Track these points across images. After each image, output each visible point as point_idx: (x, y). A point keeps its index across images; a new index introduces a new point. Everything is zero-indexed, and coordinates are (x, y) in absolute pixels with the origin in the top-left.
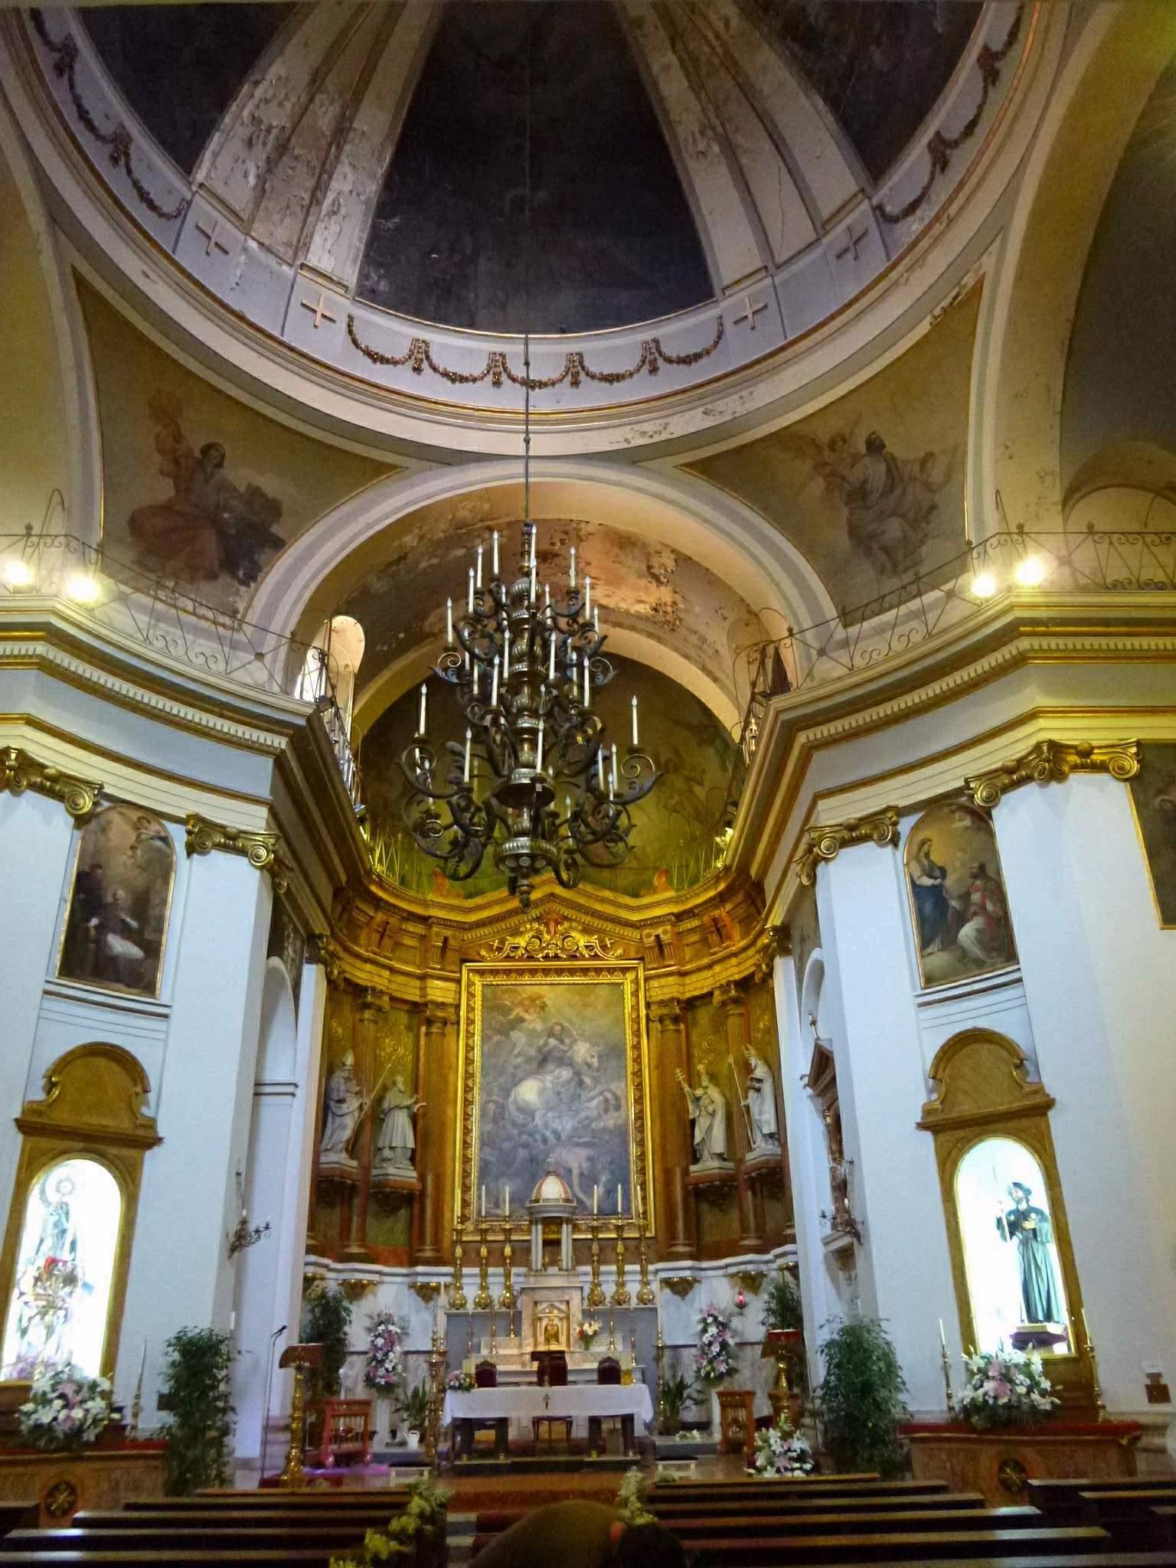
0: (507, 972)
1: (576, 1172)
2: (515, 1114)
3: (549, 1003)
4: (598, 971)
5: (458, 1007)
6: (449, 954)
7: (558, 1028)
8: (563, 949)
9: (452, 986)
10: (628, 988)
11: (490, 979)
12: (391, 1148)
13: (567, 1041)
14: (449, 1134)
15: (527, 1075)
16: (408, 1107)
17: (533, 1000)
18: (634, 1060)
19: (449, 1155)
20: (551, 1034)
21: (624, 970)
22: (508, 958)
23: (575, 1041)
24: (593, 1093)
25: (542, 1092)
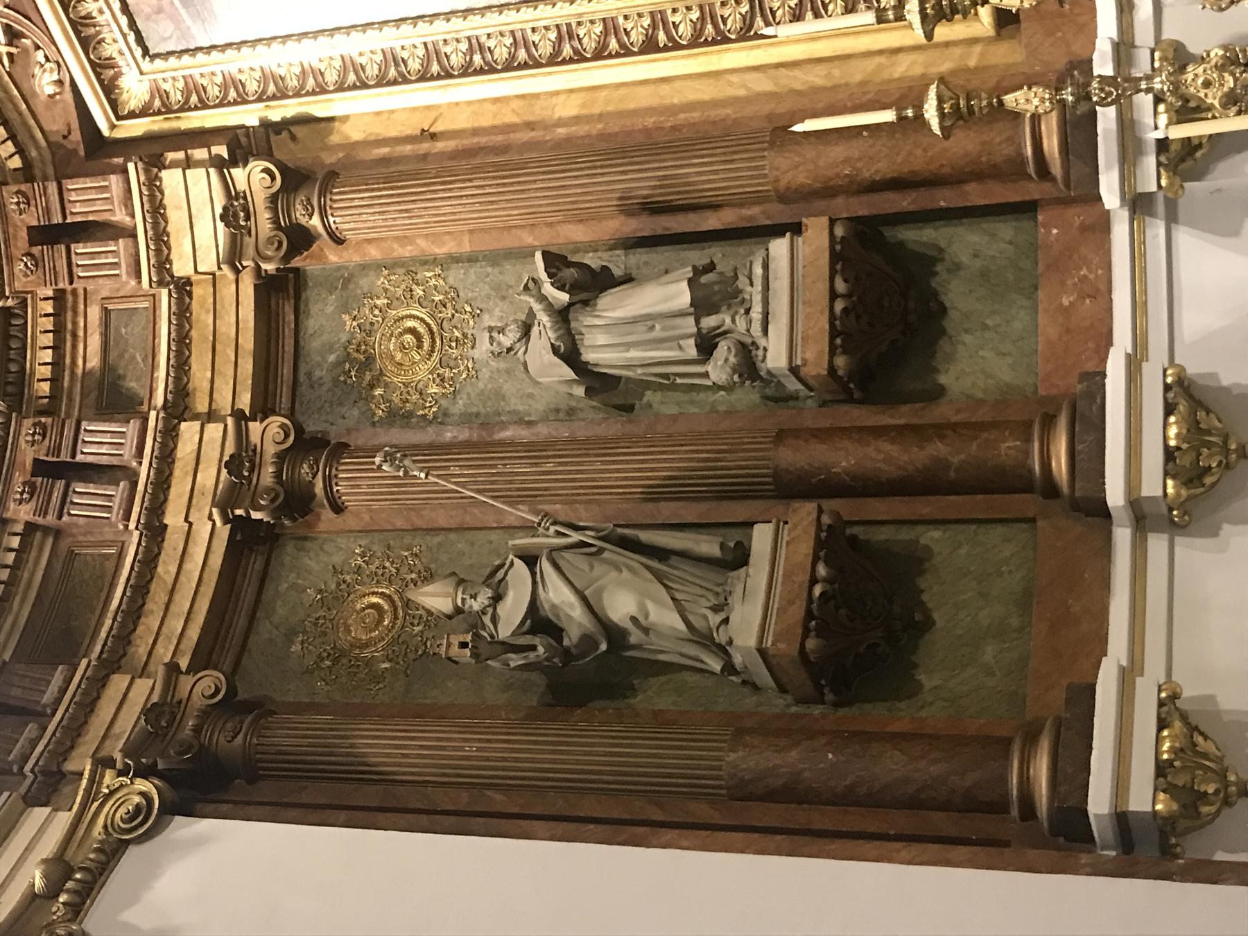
6: (79, 211)
9: (171, 179)
11: (115, 43)
12: (707, 345)
14: (644, 99)
16: (562, 316)
19: (705, 92)
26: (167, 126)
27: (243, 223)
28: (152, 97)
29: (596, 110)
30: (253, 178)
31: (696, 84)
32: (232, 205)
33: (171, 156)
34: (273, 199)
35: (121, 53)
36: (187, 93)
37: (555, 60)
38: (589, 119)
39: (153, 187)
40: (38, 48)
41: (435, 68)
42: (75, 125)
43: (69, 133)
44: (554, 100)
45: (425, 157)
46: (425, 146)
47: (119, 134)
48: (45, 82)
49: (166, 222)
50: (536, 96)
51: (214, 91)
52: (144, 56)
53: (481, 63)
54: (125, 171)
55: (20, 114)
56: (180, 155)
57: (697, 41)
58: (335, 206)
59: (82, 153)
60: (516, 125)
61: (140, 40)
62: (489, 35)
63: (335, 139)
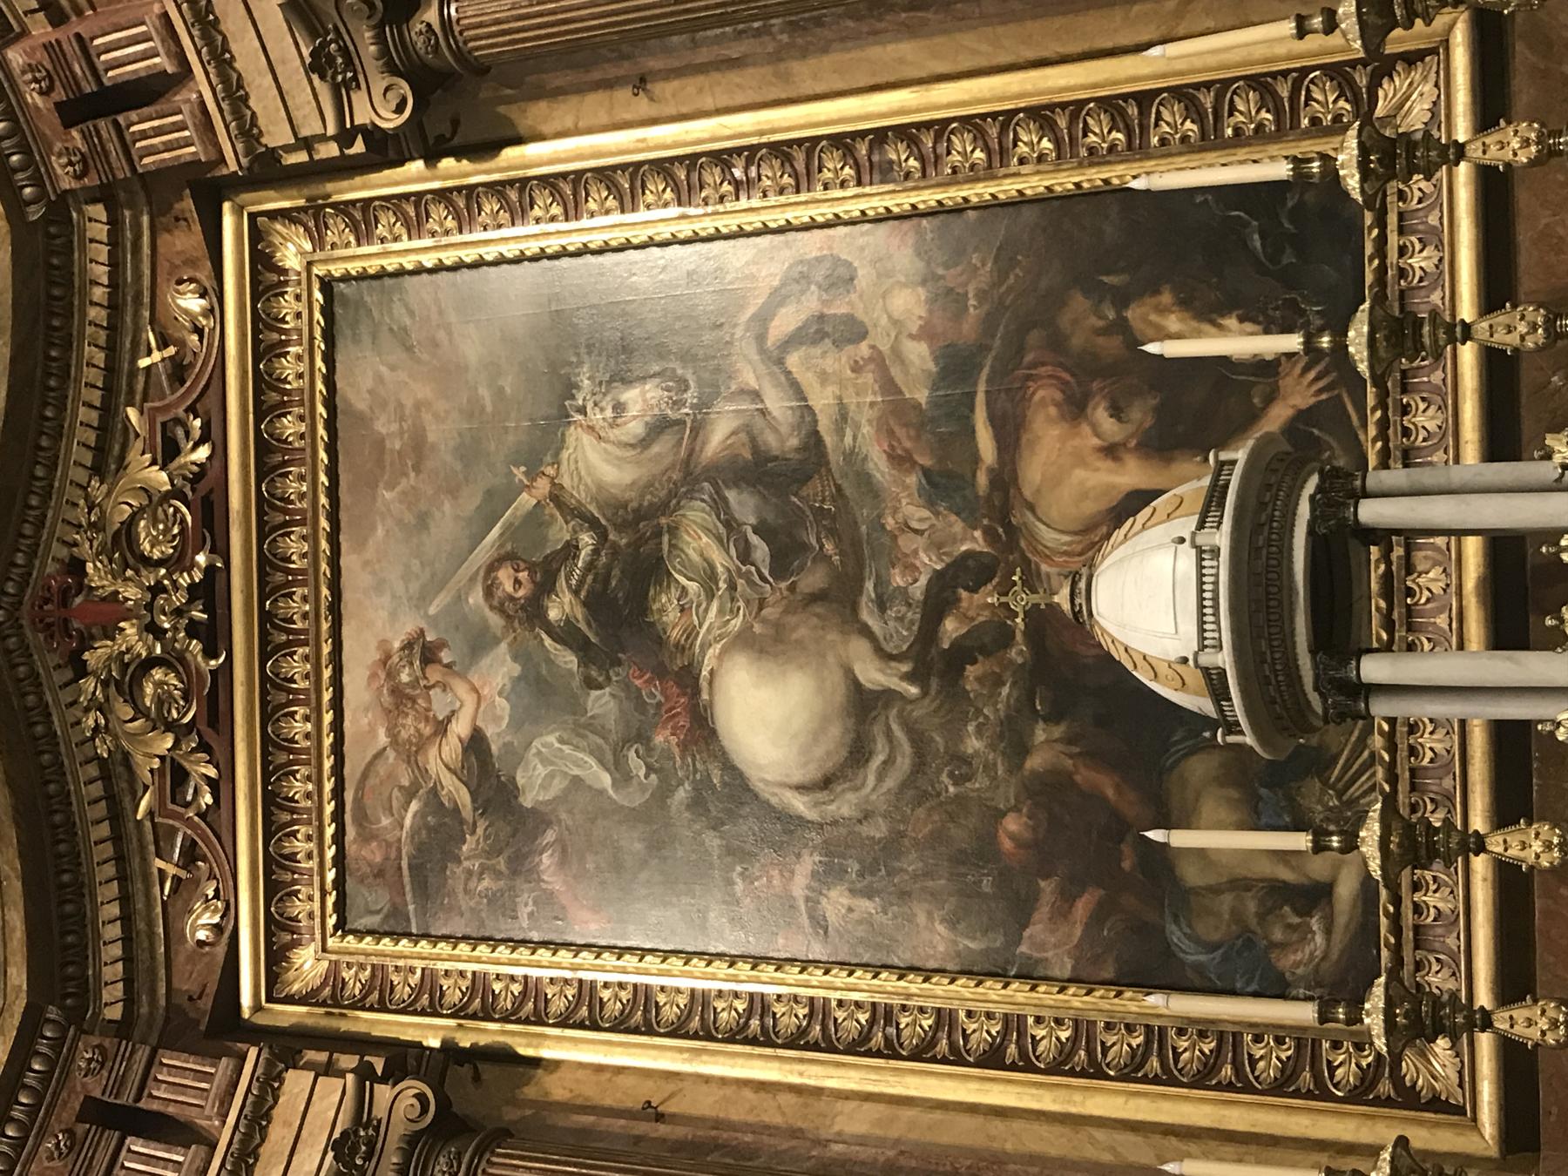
0: (273, 803)
1: (1132, 475)
2: (876, 784)
3: (408, 625)
4: (268, 398)
5: (403, 1060)
7: (505, 576)
8: (179, 561)
9: (296, 1082)
10: (353, 257)
13: (560, 532)
14: (964, 1132)
15: (702, 729)
17: (401, 699)
18: (628, 202)
20: (532, 612)
21: (265, 274)
22: (219, 819)
23: (556, 496)
24: (777, 404)
25: (767, 645)
26: (325, 1023)
27: (359, 1162)
28: (324, 984)
29: (894, 1133)
30: (400, 1103)
31: (1043, 1129)
32: (356, 1132)
33: (311, 1055)
34: (412, 1140)
35: (311, 916)
36: (367, 990)
37: (858, 1047)
38: (881, 1142)
39: (269, 1086)
40: (212, 876)
41: (695, 1023)
42: (212, 989)
43: (200, 997)
44: (839, 1105)
45: (638, 1140)
46: (642, 1128)
47: (261, 1020)
48: (201, 923)
49: (263, 1140)
50: (818, 1092)
51: (403, 992)
52: (336, 928)
53: (756, 1028)
54: (243, 1058)
55: (153, 958)
56: (322, 1057)
57: (1060, 1066)
58: (495, 1159)
59: (203, 1028)
60: (776, 1128)
61: (340, 907)
62: (779, 996)
63: (530, 1092)
